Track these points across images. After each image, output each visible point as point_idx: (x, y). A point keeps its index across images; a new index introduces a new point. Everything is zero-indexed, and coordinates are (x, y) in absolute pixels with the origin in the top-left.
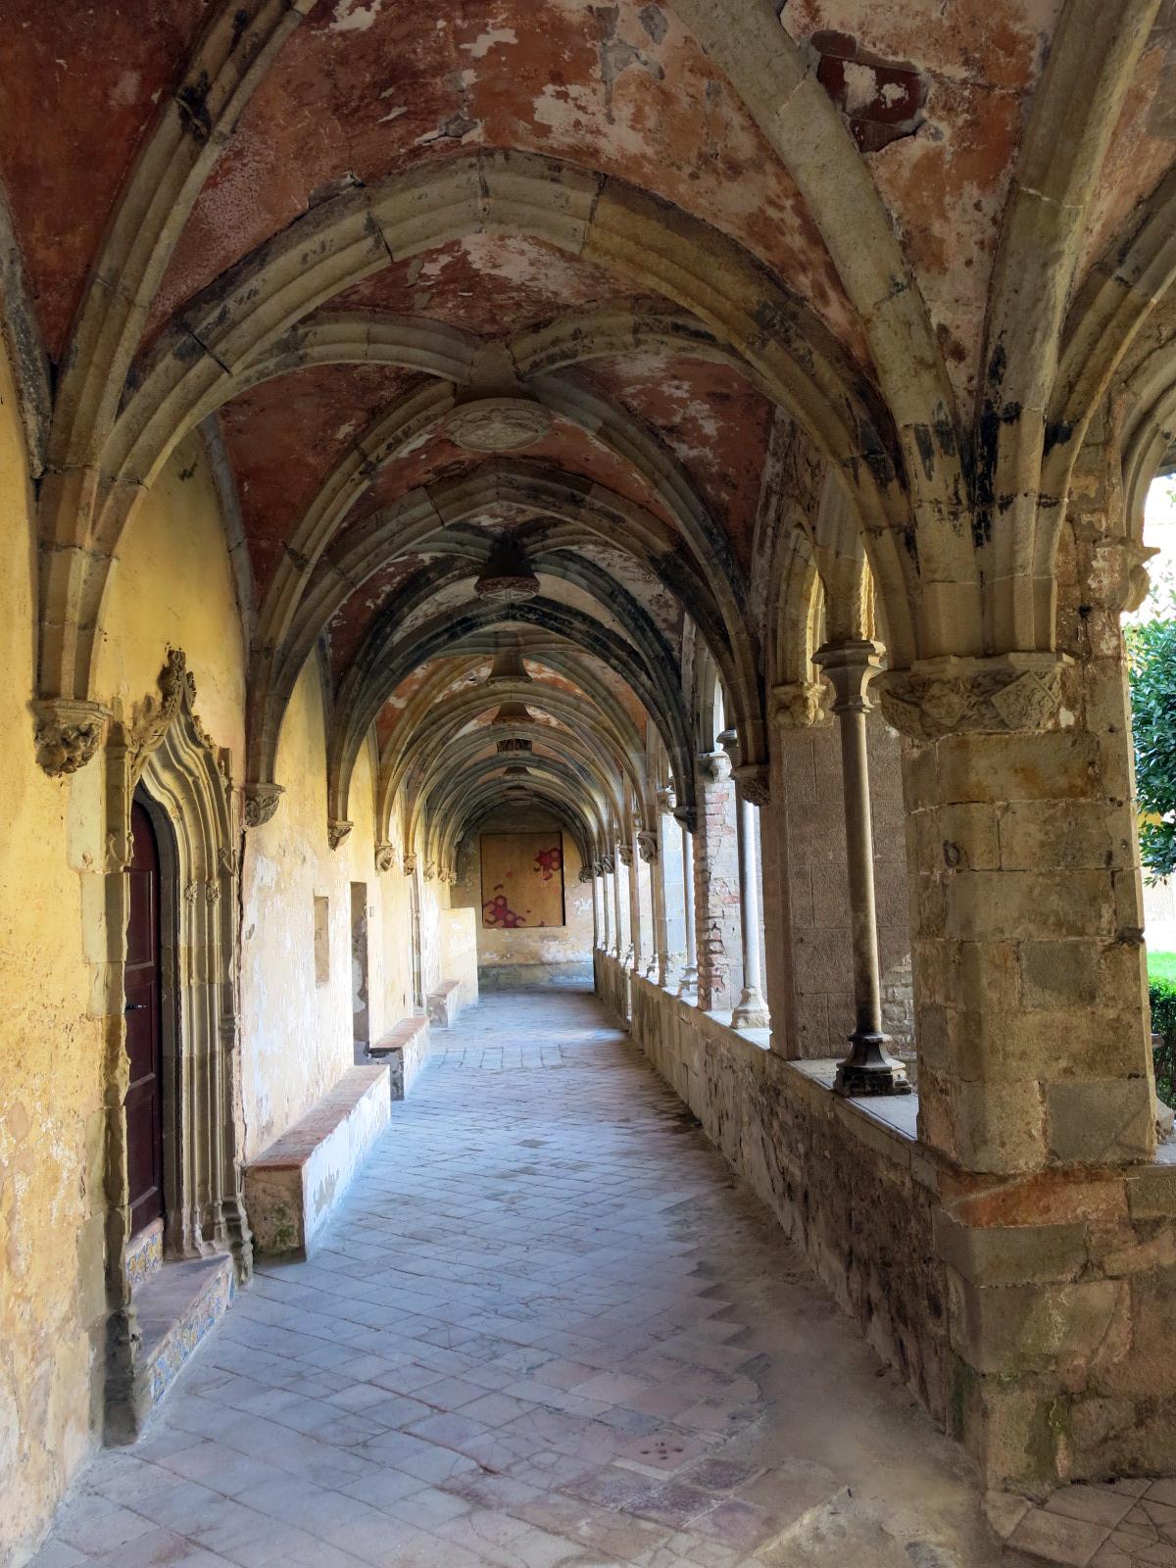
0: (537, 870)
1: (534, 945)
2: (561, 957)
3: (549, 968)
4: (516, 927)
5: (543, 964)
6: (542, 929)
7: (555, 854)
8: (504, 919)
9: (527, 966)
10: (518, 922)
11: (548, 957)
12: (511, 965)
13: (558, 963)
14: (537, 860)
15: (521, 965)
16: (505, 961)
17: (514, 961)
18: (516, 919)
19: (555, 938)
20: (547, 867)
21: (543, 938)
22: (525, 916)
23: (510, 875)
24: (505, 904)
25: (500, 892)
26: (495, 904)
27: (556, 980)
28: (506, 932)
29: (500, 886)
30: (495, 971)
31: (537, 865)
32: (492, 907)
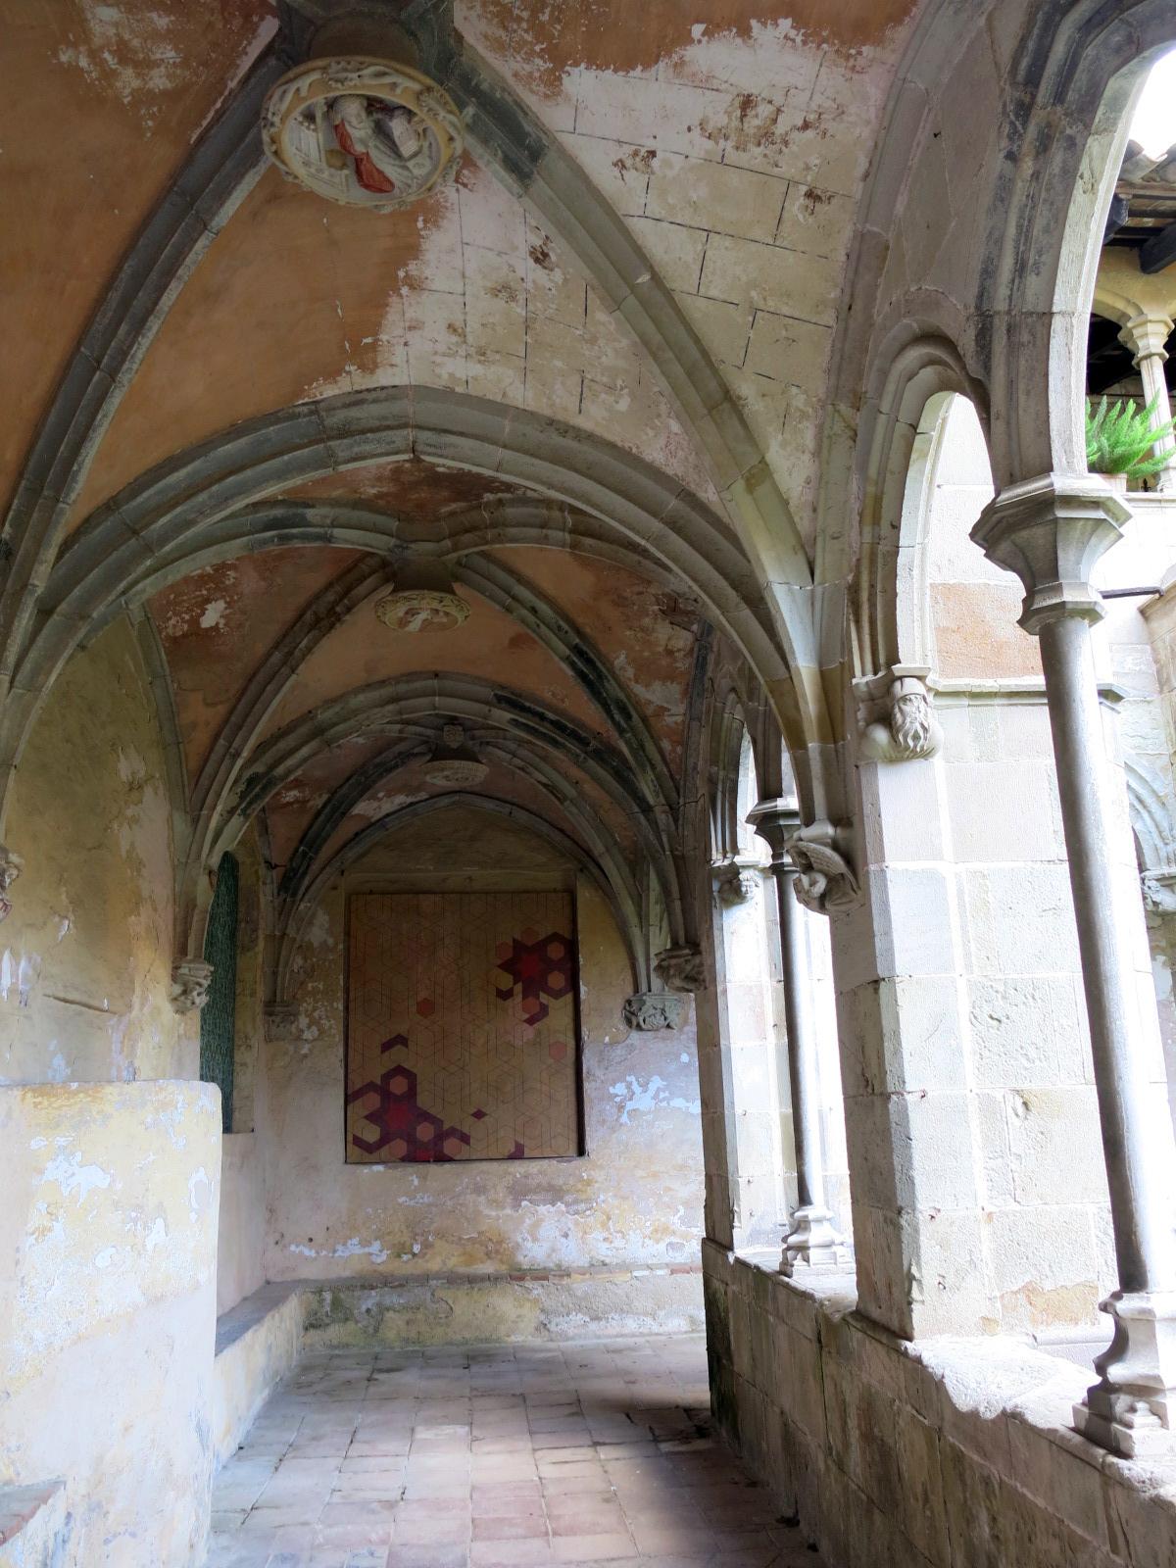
0: (505, 995)
1: (495, 1215)
2: (571, 1253)
3: (537, 1290)
4: (442, 1159)
5: (518, 1275)
6: (518, 1168)
7: (556, 952)
8: (411, 1139)
9: (472, 1280)
10: (450, 1146)
11: (534, 1251)
12: (424, 1279)
13: (564, 1272)
14: (506, 966)
15: (453, 1279)
16: (406, 1266)
17: (434, 1265)
18: (441, 1136)
19: (555, 1194)
20: (533, 985)
21: (519, 1193)
22: (468, 1126)
23: (426, 1008)
24: (412, 1092)
25: (398, 1056)
26: (384, 1092)
27: (560, 1325)
28: (413, 1176)
29: (401, 1040)
30: (370, 1300)
31: (506, 980)
32: (373, 1101)
